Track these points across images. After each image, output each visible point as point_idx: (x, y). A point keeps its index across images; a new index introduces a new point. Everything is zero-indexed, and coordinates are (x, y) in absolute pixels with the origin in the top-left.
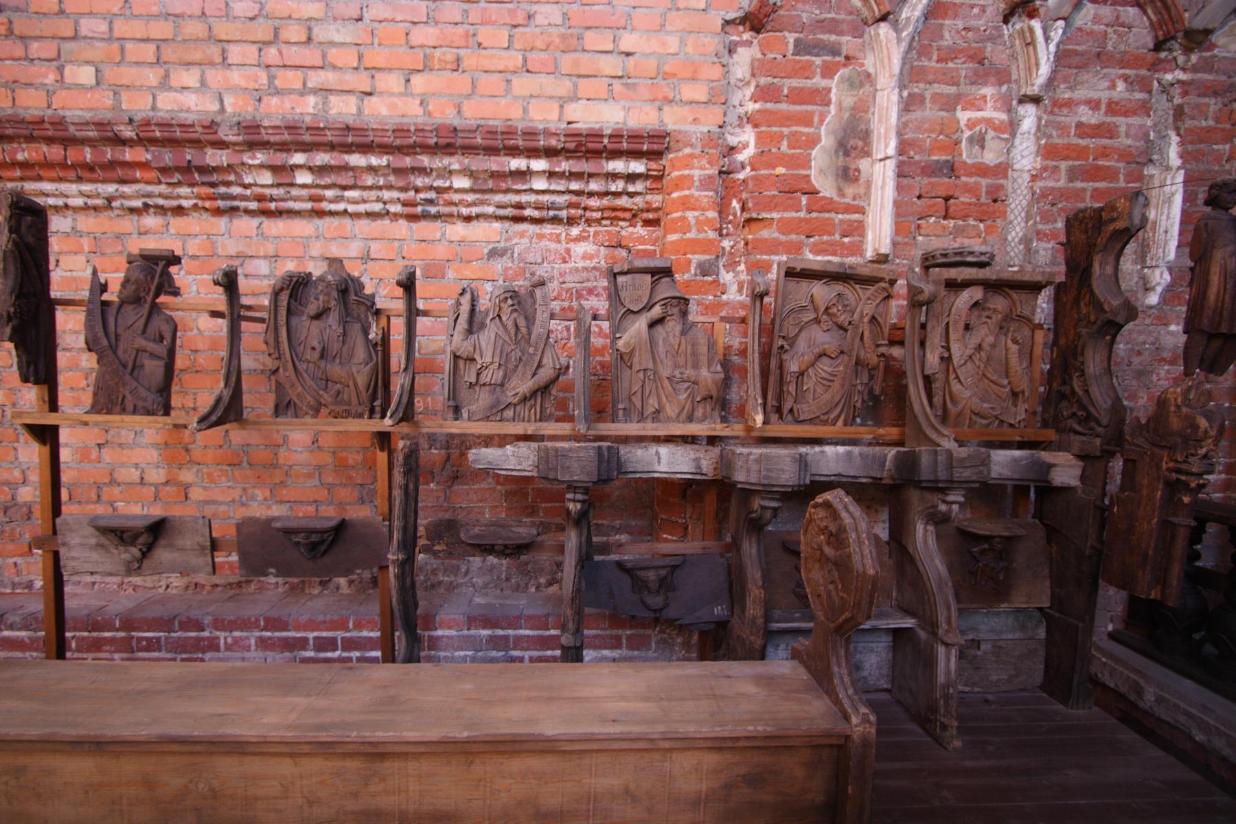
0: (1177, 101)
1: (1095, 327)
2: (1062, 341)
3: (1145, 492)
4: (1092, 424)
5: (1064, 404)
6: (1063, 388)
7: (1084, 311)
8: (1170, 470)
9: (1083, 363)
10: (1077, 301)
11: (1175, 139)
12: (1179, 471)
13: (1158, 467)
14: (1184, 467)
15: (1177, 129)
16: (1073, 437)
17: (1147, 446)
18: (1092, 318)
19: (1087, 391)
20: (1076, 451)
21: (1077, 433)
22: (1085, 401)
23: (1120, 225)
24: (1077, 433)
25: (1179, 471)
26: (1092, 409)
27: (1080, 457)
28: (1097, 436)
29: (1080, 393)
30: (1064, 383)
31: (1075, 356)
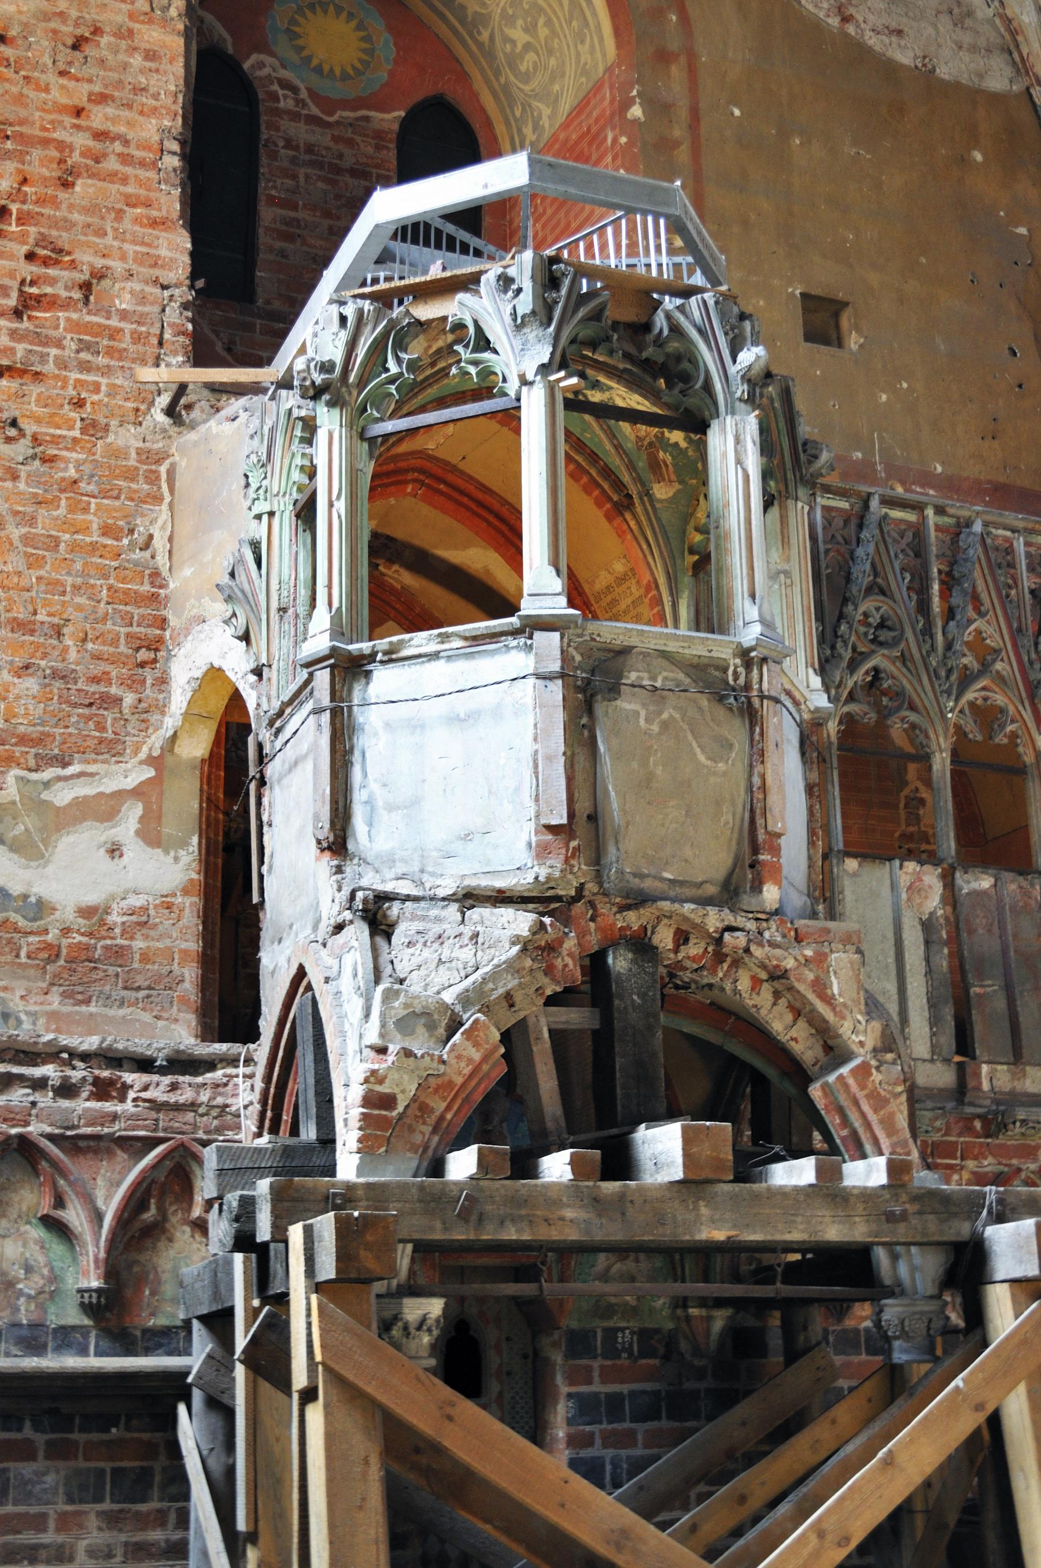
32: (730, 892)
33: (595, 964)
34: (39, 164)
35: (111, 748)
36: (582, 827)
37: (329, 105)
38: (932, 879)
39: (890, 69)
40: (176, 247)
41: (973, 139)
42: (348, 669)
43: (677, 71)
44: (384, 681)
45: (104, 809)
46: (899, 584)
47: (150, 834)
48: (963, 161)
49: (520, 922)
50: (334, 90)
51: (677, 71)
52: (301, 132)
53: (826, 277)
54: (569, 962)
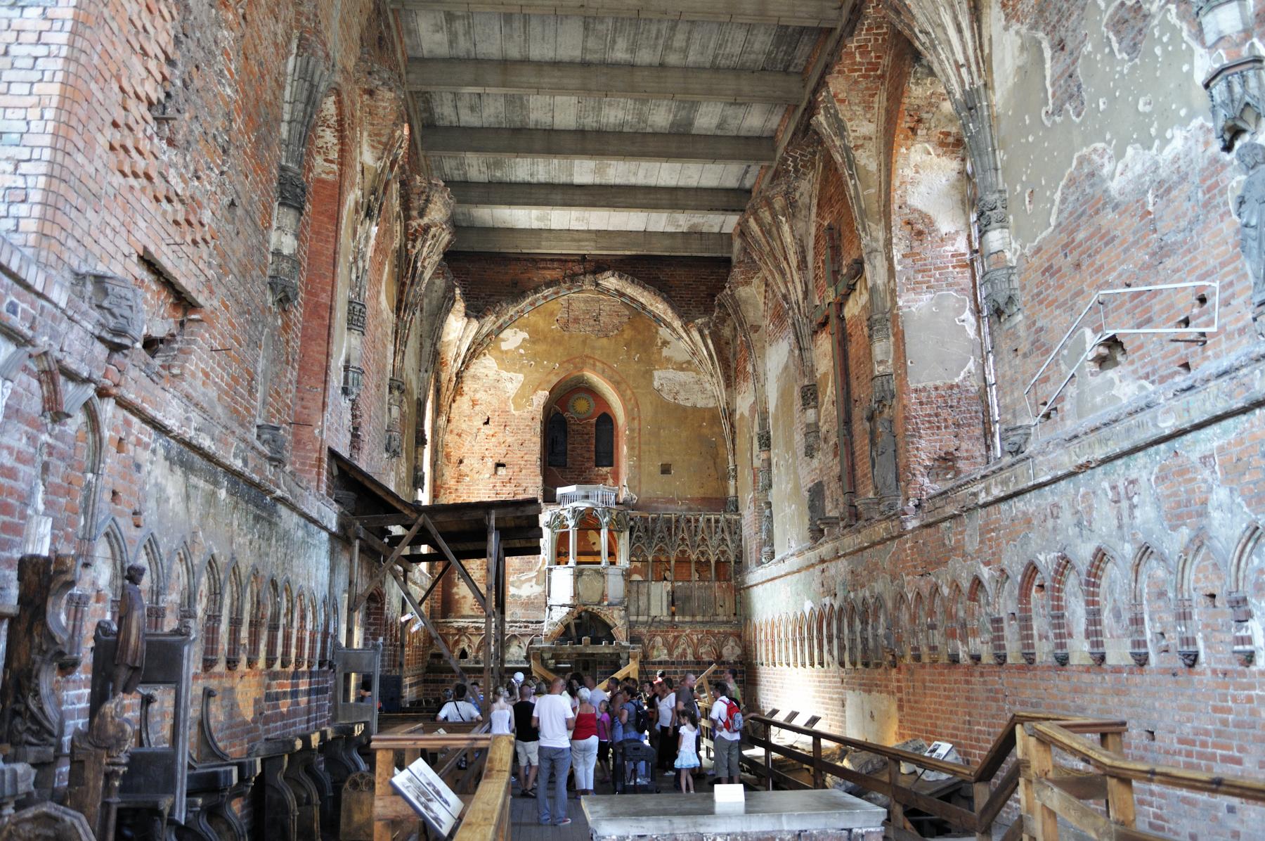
0: (45, 458)
1: (49, 656)
2: (15, 665)
3: (91, 784)
4: (46, 736)
5: (18, 720)
6: (18, 707)
7: (37, 640)
8: (108, 764)
9: (37, 685)
10: (29, 631)
11: (42, 488)
12: (114, 764)
13: (100, 763)
14: (116, 760)
15: (44, 480)
16: (28, 748)
17: (92, 749)
18: (44, 647)
19: (41, 709)
20: (32, 759)
21: (31, 744)
22: (40, 716)
23: (68, 577)
24: (31, 744)
25: (114, 764)
26: (46, 724)
27: (34, 765)
28: (51, 745)
29: (35, 709)
30: (17, 701)
31: (29, 678)
32: (599, 603)
33: (580, 614)
34: (516, 469)
35: (531, 570)
36: (576, 595)
37: (581, 420)
38: (669, 584)
39: (684, 409)
40: (539, 479)
41: (703, 419)
42: (550, 570)
43: (636, 422)
44: (553, 573)
45: (530, 580)
46: (665, 530)
47: (537, 583)
48: (701, 426)
49: (567, 609)
50: (582, 417)
51: (636, 422)
52: (575, 427)
53: (666, 459)
54: (576, 614)
